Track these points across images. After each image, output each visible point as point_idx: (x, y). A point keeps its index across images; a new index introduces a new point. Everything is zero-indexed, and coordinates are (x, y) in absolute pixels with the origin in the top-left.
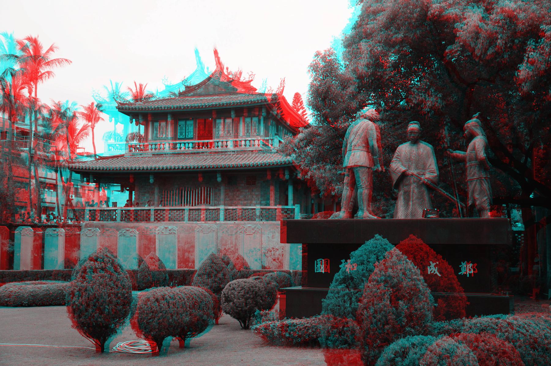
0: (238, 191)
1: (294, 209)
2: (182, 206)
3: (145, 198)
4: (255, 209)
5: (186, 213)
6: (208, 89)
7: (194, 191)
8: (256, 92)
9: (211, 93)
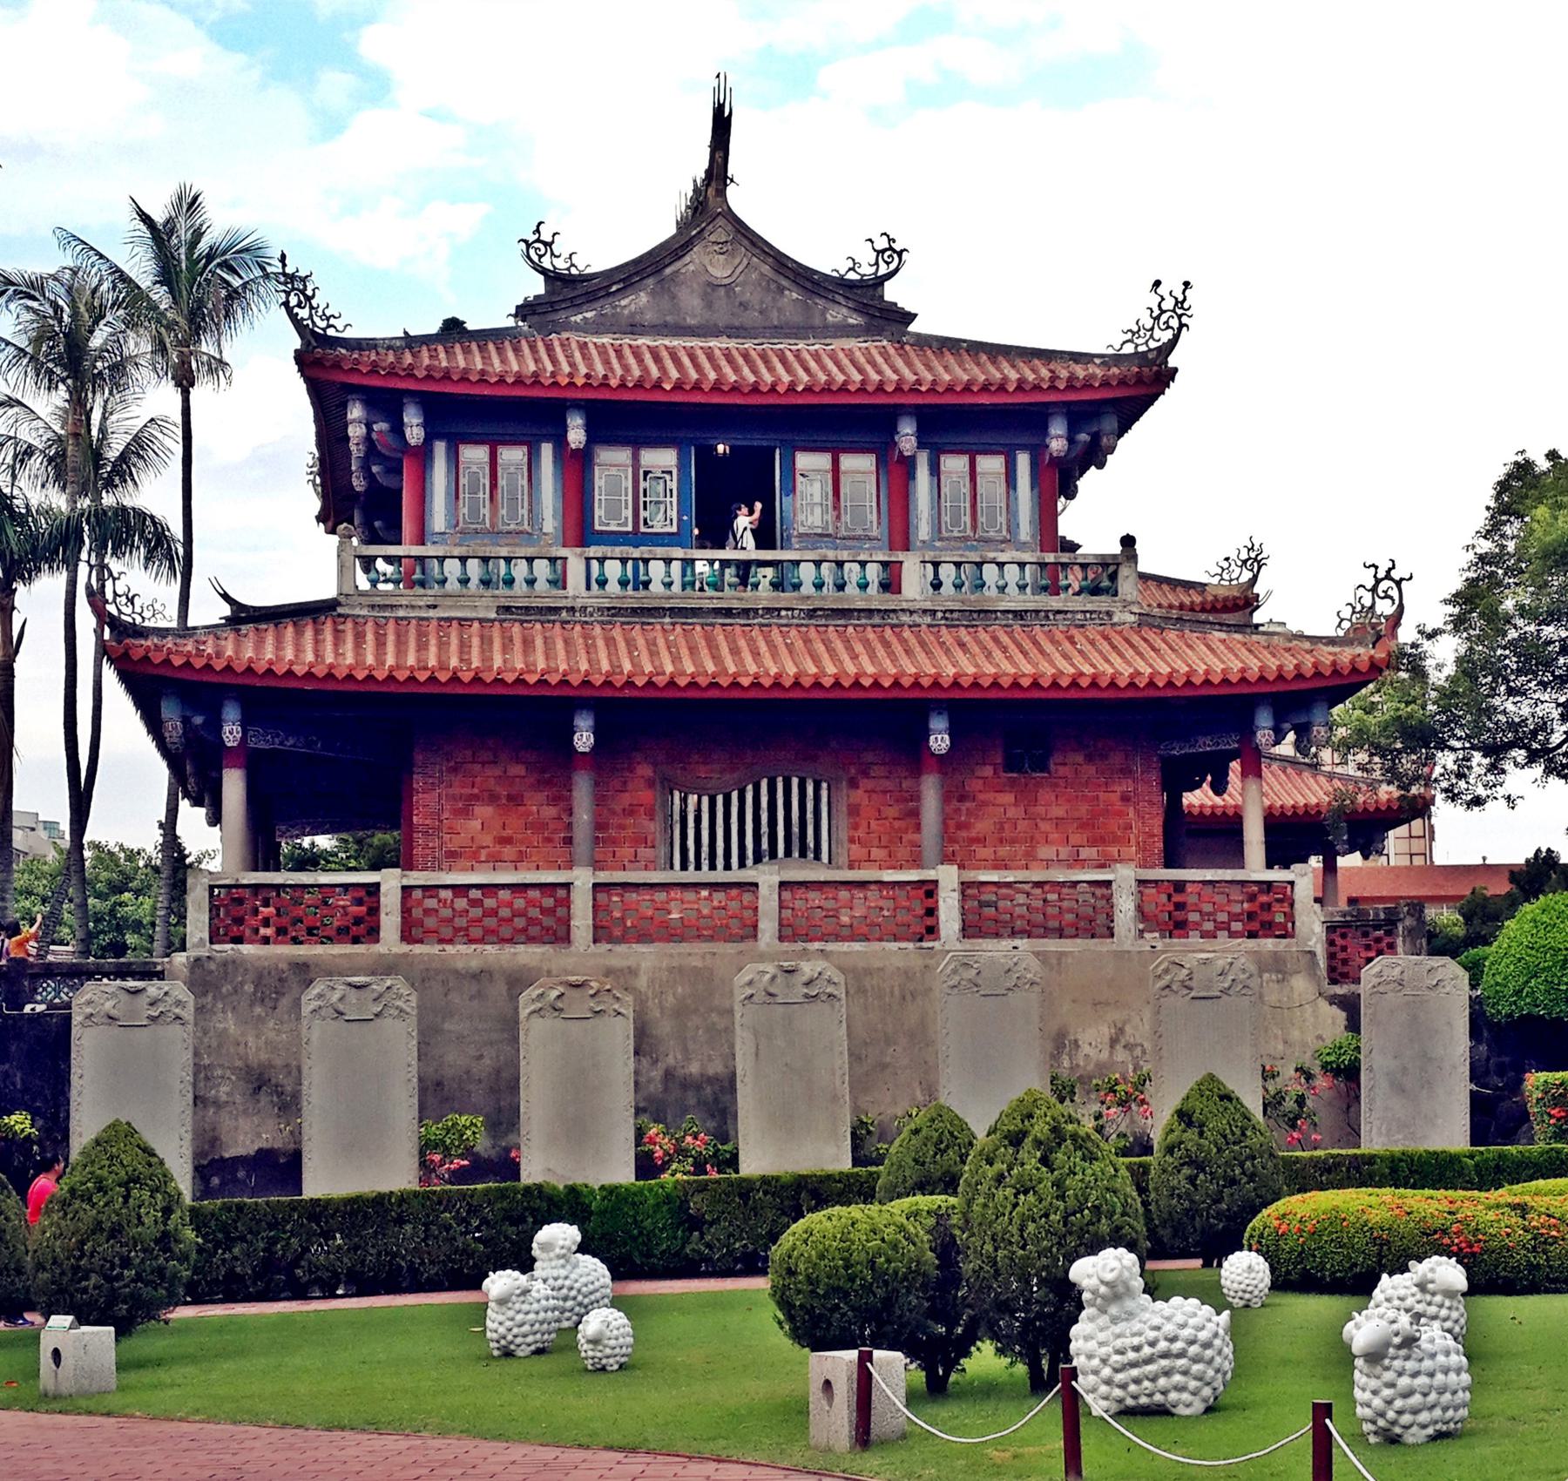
0: (962, 799)
1: (1292, 883)
2: (672, 867)
3: (476, 824)
4: (1108, 884)
5: (768, 900)
6: (674, 297)
7: (735, 795)
8: (913, 328)
9: (690, 321)
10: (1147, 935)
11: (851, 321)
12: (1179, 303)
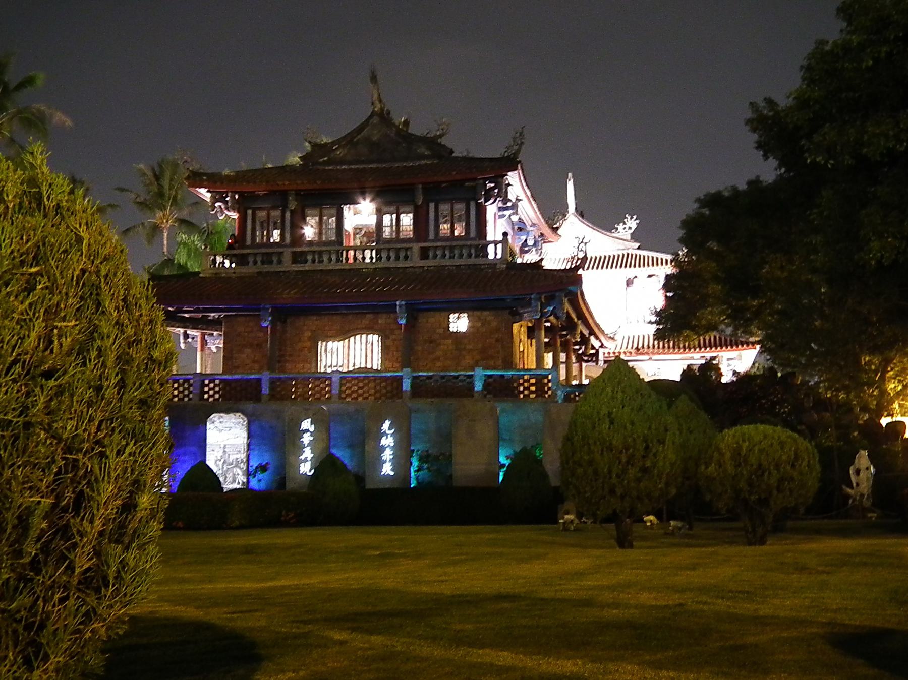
3: (244, 356)
10: (488, 396)
11: (426, 153)
12: (521, 134)
